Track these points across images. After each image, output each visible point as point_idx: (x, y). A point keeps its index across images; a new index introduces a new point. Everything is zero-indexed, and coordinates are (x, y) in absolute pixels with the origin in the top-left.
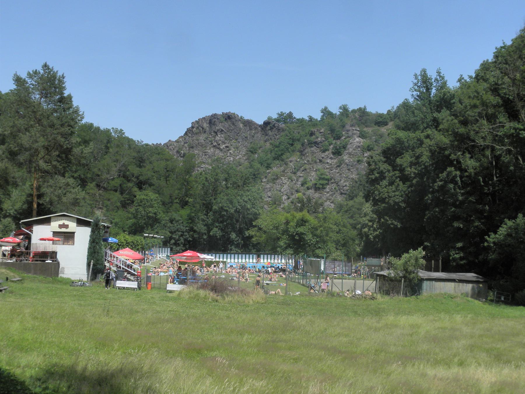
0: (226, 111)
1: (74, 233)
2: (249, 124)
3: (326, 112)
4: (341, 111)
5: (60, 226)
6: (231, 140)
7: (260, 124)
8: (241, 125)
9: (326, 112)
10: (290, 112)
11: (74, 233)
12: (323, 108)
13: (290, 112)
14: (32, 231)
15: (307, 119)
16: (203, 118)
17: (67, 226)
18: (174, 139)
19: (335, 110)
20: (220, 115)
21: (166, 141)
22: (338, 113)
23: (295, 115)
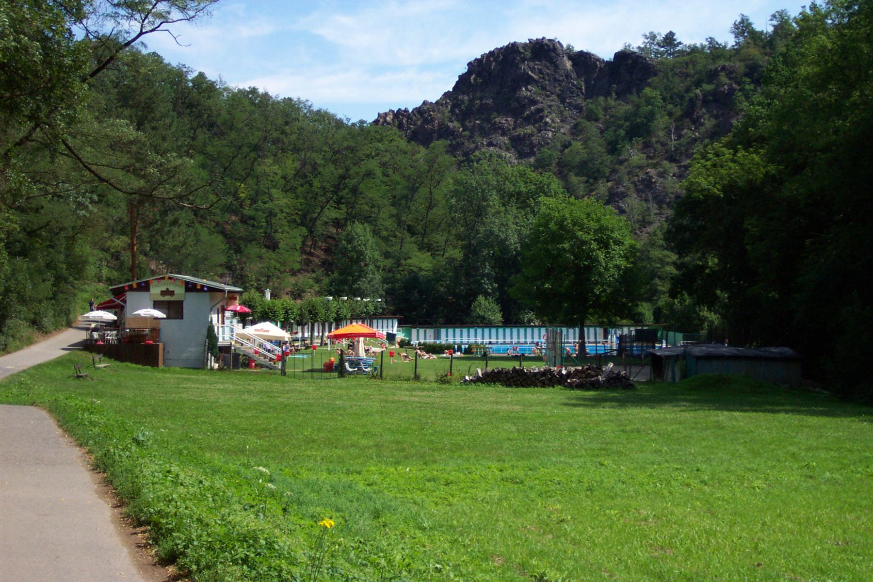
0: (536, 35)
1: (181, 302)
2: (583, 60)
3: (743, 28)
4: (775, 23)
5: (163, 293)
6: (548, 96)
7: (606, 59)
8: (568, 64)
9: (743, 28)
10: (671, 32)
11: (181, 302)
12: (739, 20)
13: (671, 32)
14: (125, 301)
15: (706, 43)
16: (490, 52)
17: (172, 293)
18: (434, 97)
19: (764, 25)
20: (525, 44)
21: (419, 104)
22: (770, 29)
23: (678, 38)
